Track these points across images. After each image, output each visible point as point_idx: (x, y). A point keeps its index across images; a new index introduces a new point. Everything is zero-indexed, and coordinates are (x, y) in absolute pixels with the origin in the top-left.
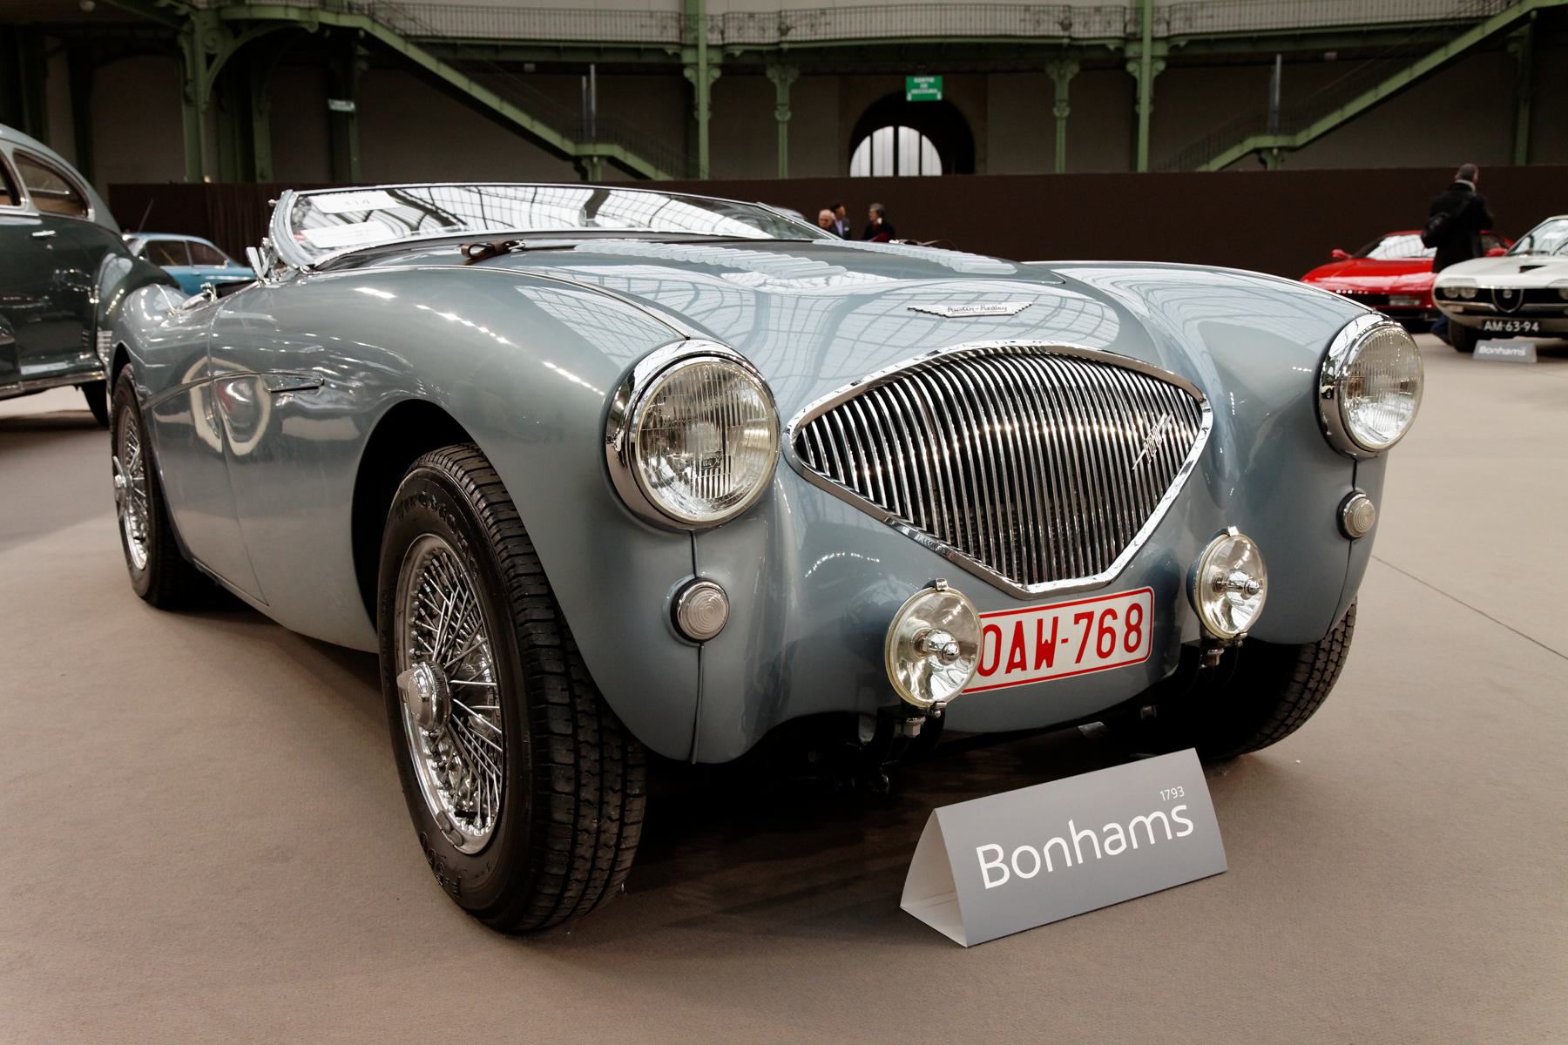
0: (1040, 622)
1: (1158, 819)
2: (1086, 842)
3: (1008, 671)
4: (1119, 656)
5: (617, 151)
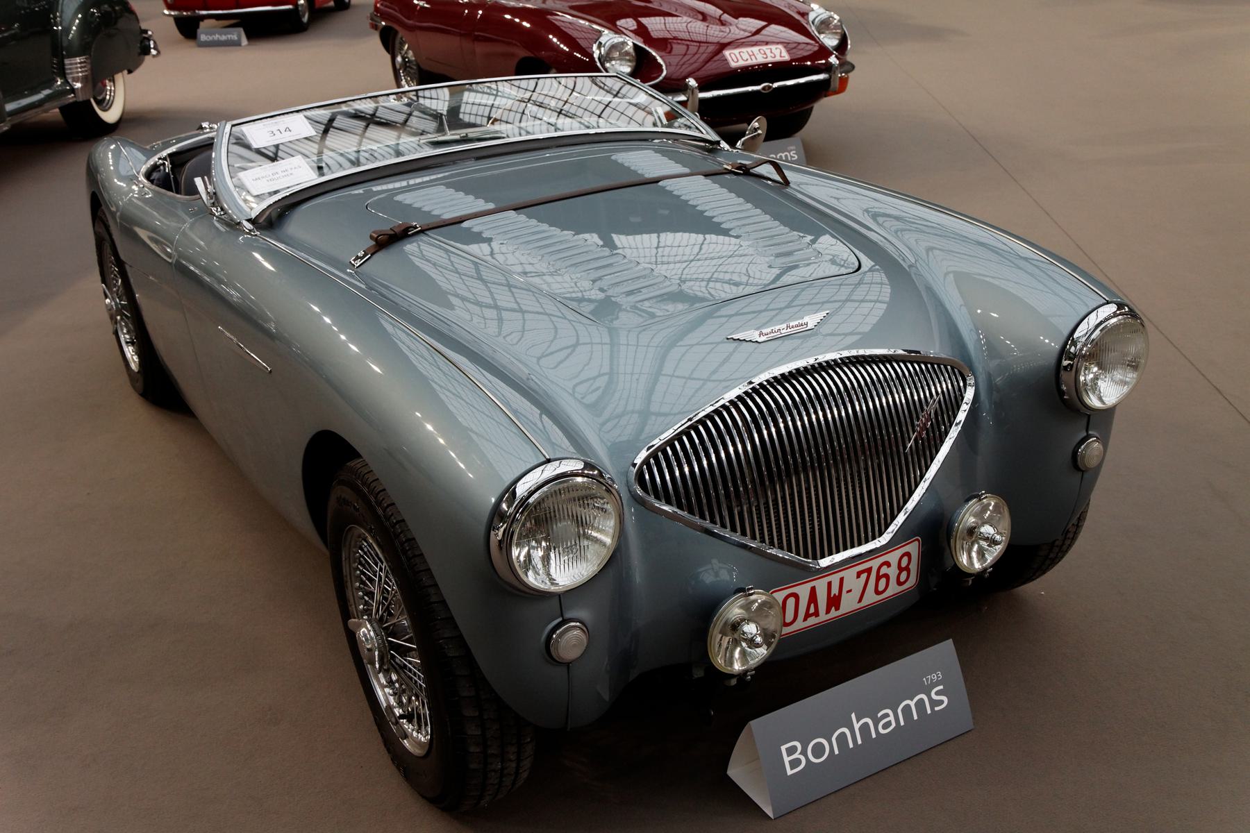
0: (830, 584)
1: (922, 700)
2: (865, 728)
3: (805, 619)
4: (893, 589)
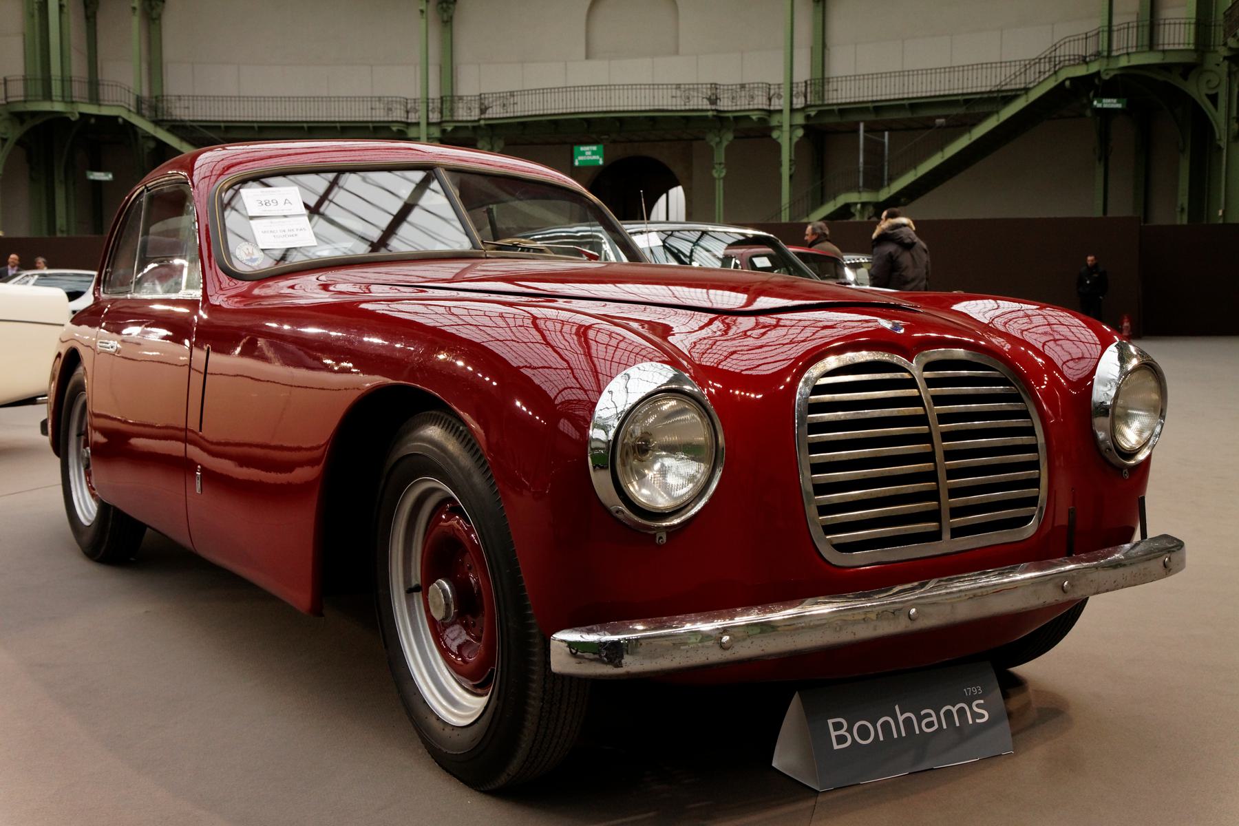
2: (908, 722)
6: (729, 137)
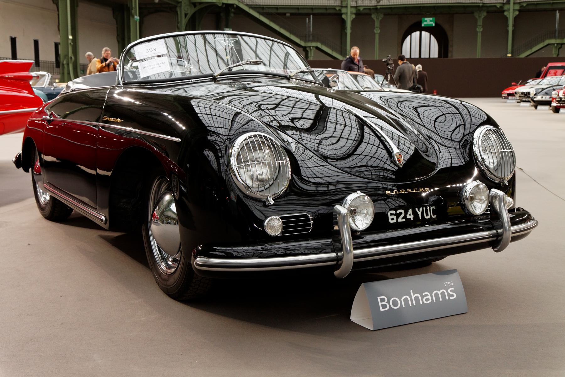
2: (417, 298)
5: (319, 45)
6: (484, 14)
